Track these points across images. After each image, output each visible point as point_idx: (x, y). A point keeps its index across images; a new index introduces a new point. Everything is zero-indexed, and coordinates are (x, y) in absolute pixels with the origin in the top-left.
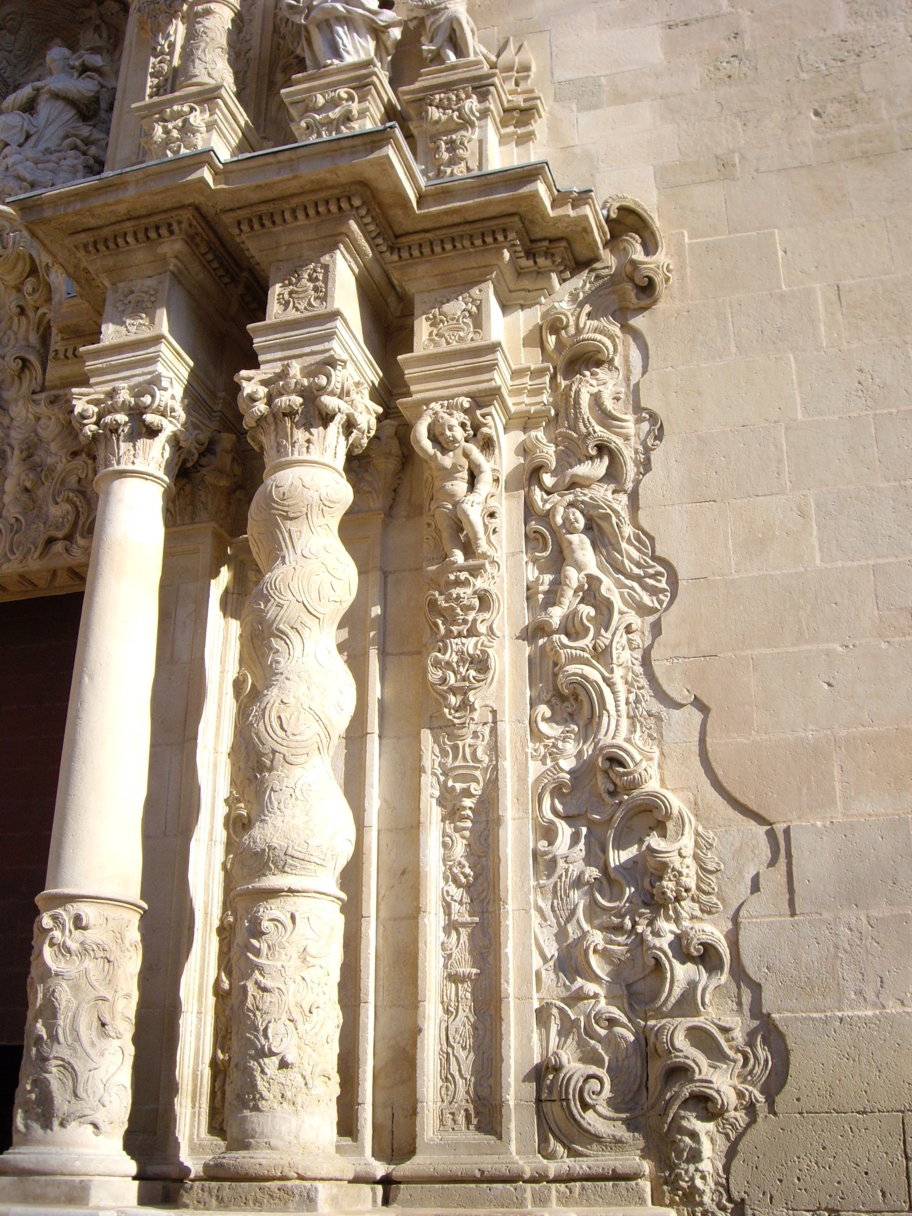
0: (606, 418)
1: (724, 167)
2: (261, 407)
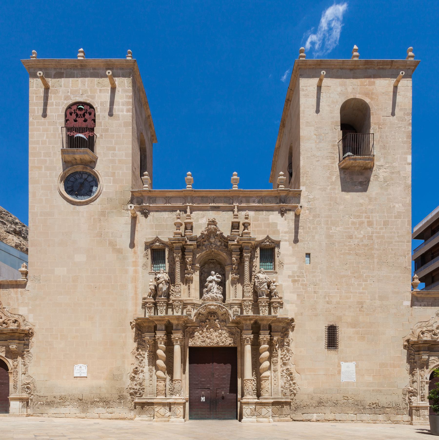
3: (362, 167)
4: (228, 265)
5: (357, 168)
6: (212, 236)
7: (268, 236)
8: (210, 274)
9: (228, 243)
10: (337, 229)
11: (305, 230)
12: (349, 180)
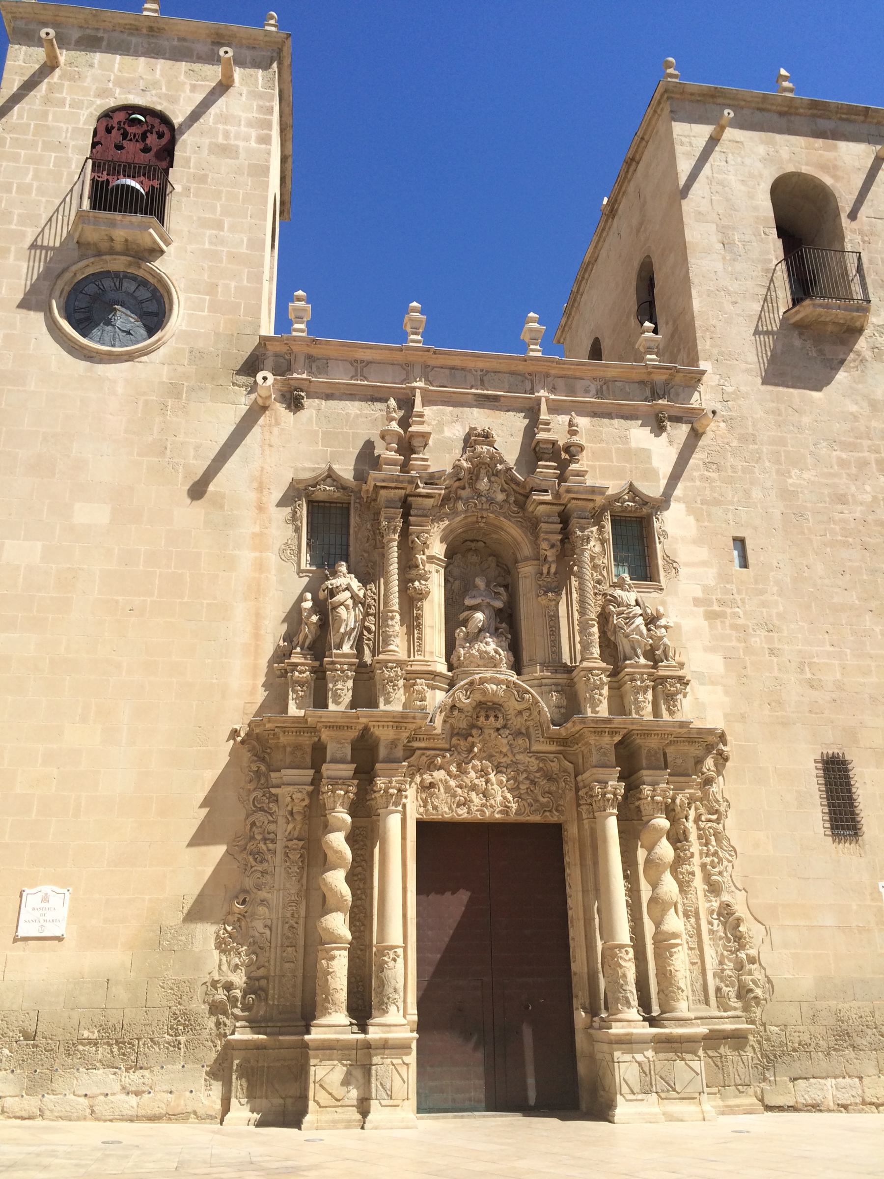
0: (717, 801)
1: (743, 717)
3: (843, 324)
4: (526, 559)
5: (830, 328)
6: (483, 471)
7: (631, 485)
10: (806, 475)
11: (723, 473)
12: (815, 355)
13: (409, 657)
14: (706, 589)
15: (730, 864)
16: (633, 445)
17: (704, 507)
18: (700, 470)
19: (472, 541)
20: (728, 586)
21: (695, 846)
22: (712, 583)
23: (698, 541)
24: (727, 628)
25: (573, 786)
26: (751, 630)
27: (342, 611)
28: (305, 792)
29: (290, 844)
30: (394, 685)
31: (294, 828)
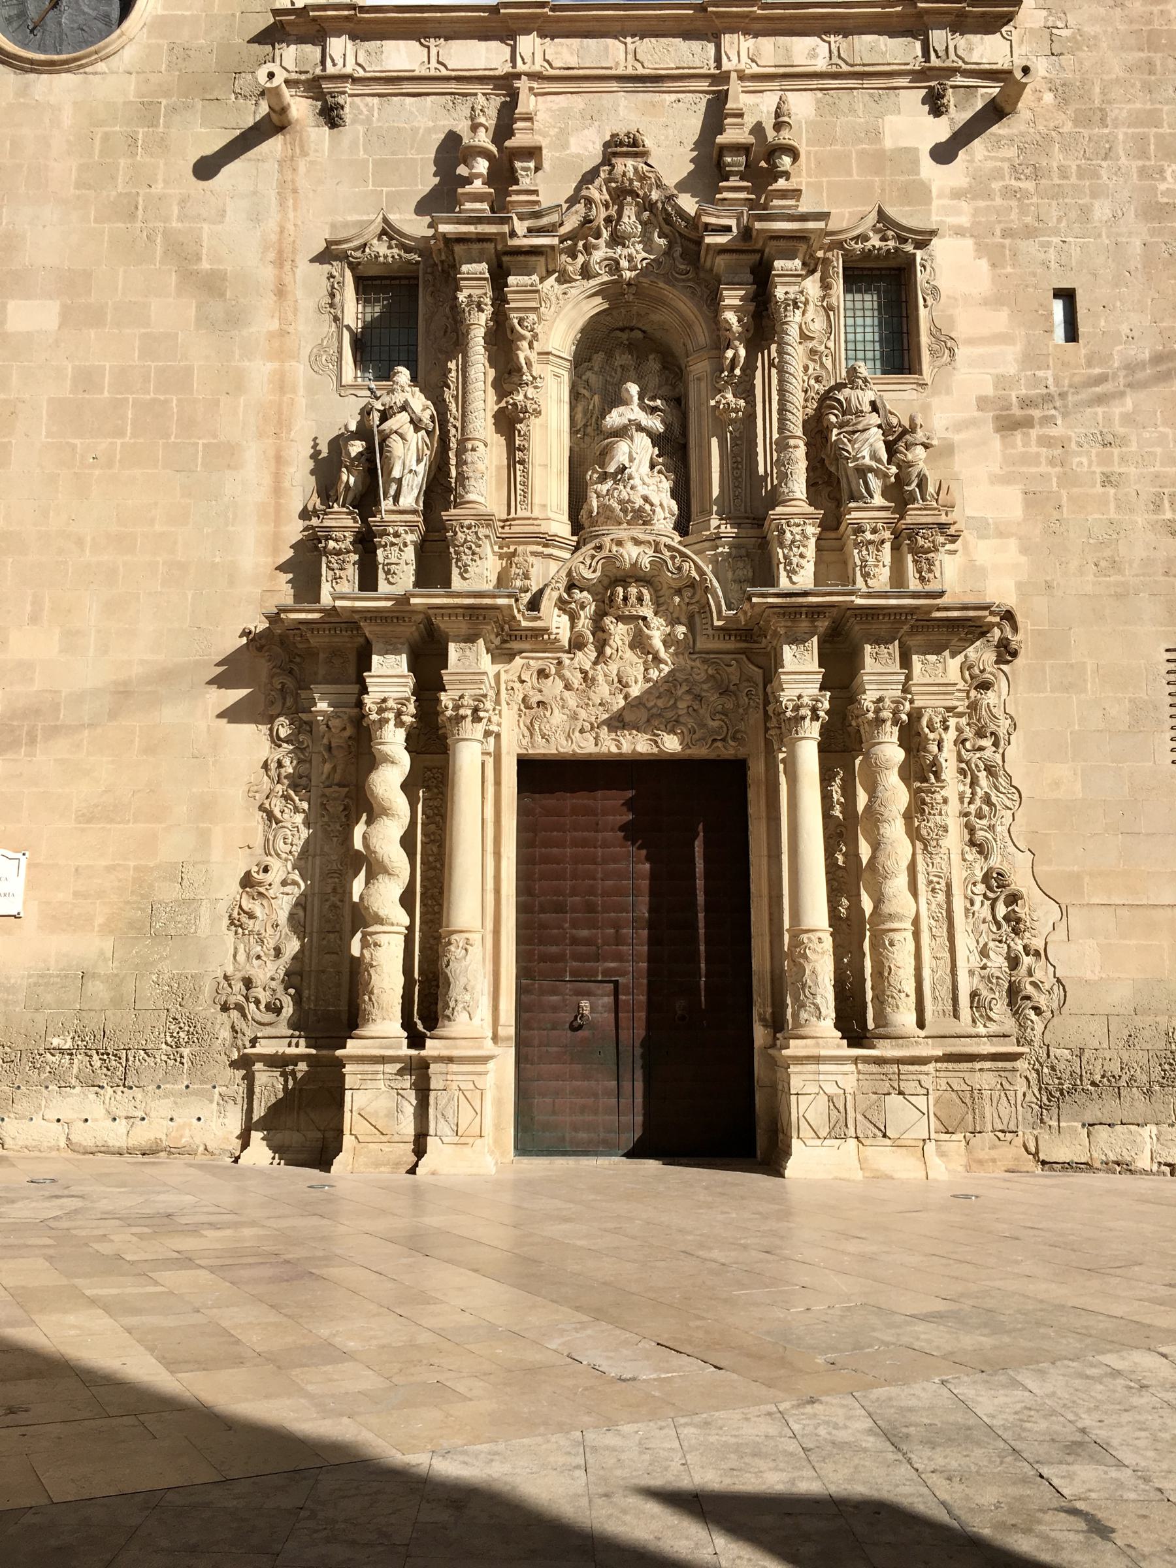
2: (871, 715)
8: (618, 400)
9: (699, 242)
11: (1043, 181)
13: (509, 514)
14: (1001, 381)
15: (1010, 813)
16: (888, 144)
17: (1007, 242)
18: (1003, 178)
19: (622, 330)
20: (1040, 374)
21: (952, 785)
22: (1012, 369)
23: (995, 301)
24: (1033, 443)
25: (761, 702)
26: (1073, 446)
27: (395, 444)
28: (346, 717)
29: (328, 791)
30: (473, 554)
31: (334, 768)
